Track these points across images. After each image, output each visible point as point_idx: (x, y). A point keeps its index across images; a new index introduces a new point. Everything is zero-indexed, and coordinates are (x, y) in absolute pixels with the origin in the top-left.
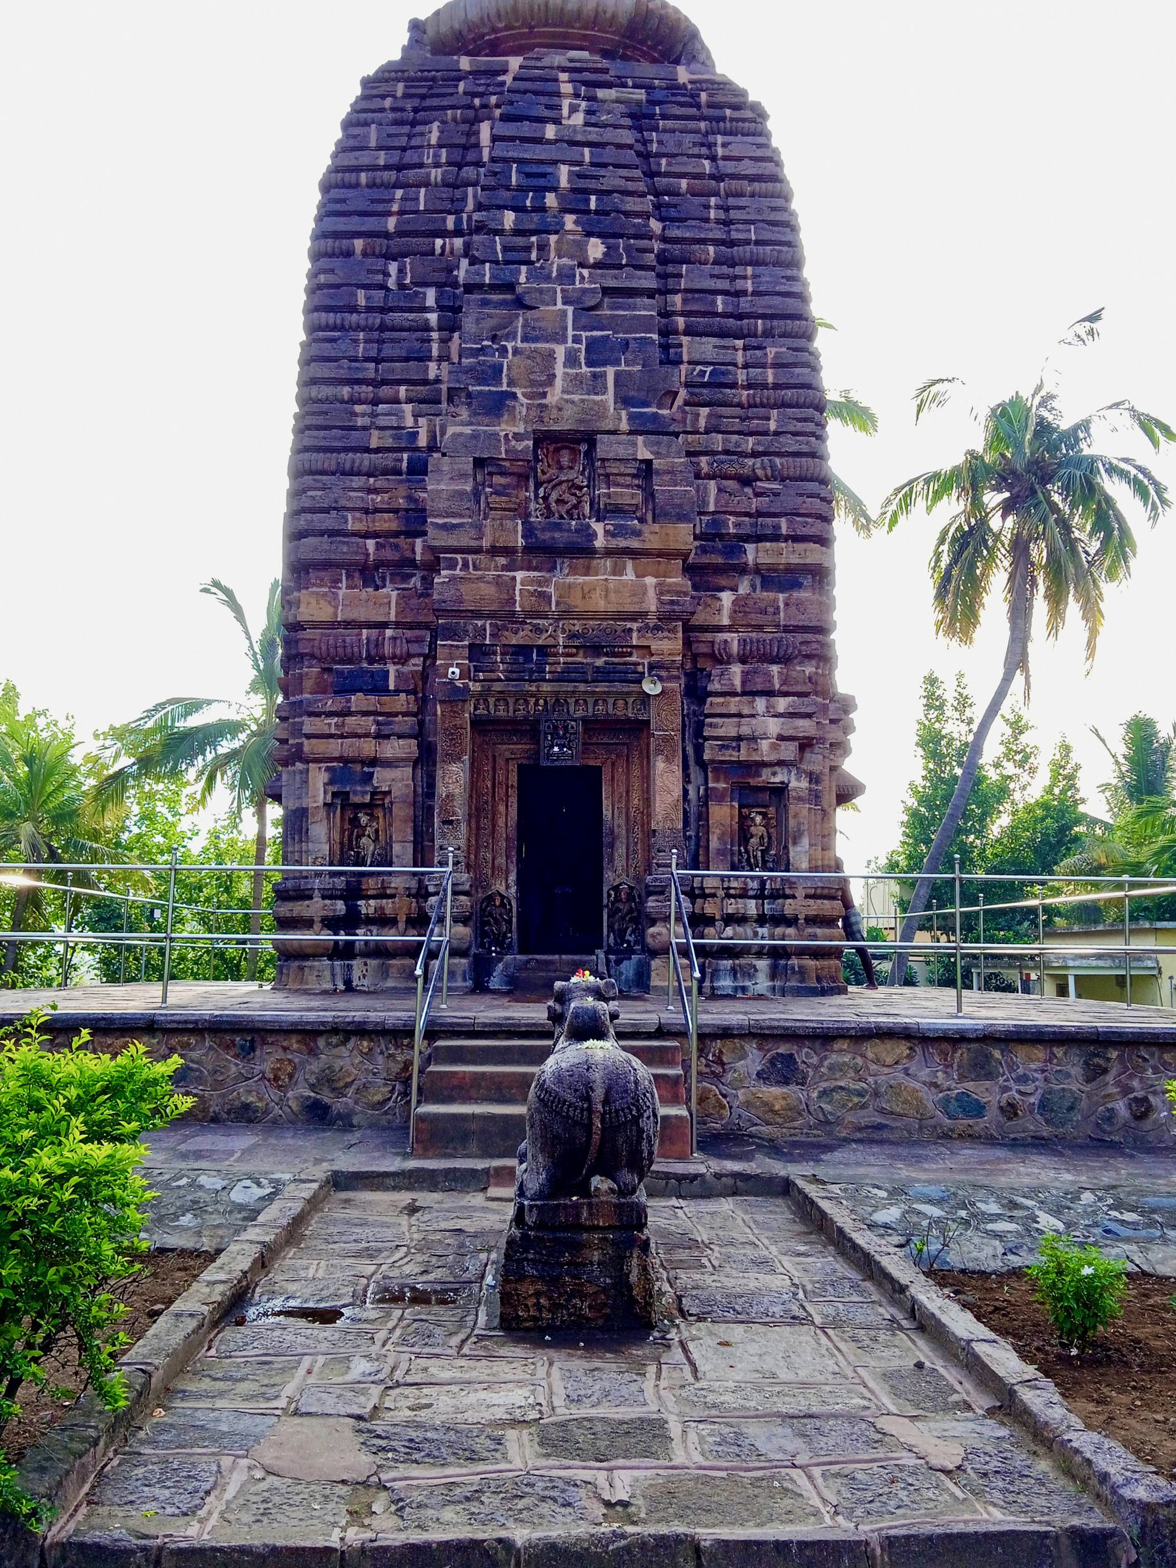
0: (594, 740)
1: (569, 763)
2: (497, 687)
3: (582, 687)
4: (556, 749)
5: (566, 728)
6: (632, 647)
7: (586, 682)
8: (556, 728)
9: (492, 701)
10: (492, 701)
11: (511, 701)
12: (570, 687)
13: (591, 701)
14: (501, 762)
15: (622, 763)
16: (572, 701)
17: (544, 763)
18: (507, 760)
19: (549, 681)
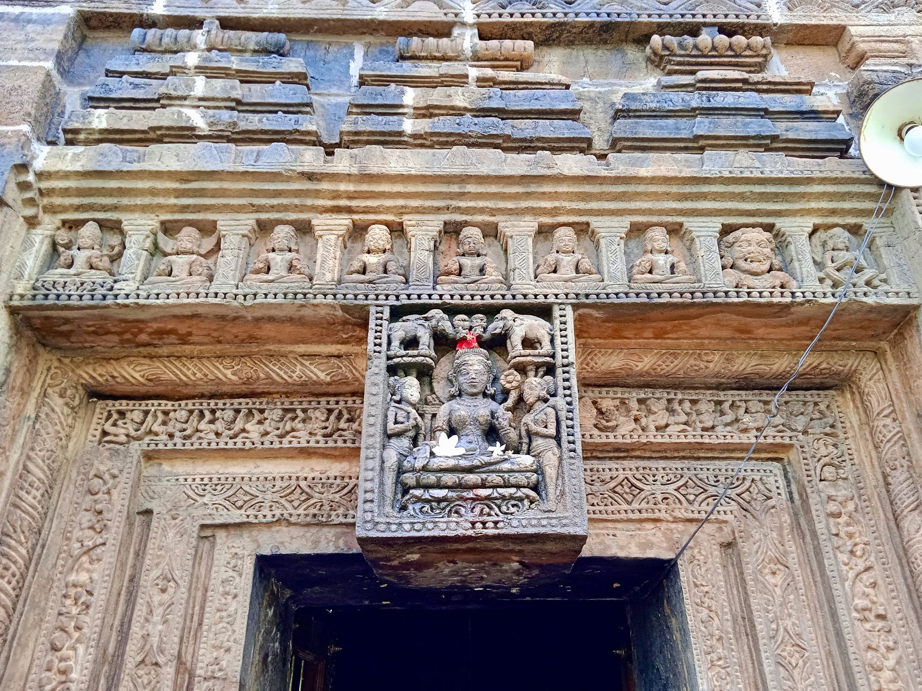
0: (625, 431)
1: (524, 521)
2: (169, 158)
3: (571, 164)
4: (447, 449)
5: (496, 344)
6: (761, 30)
7: (583, 146)
8: (444, 343)
9: (139, 228)
10: (139, 228)
11: (234, 228)
12: (517, 164)
13: (610, 229)
14: (170, 545)
15: (766, 538)
16: (520, 230)
17: (379, 519)
18: (208, 531)
19: (421, 141)
